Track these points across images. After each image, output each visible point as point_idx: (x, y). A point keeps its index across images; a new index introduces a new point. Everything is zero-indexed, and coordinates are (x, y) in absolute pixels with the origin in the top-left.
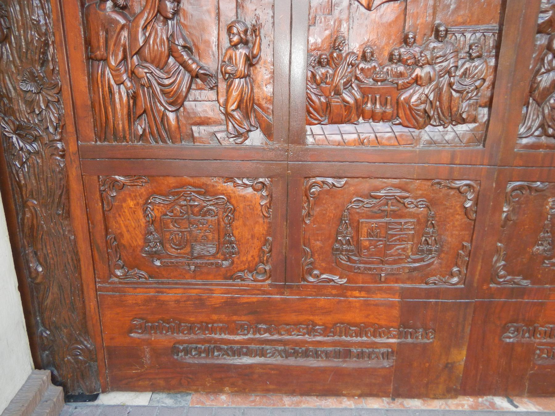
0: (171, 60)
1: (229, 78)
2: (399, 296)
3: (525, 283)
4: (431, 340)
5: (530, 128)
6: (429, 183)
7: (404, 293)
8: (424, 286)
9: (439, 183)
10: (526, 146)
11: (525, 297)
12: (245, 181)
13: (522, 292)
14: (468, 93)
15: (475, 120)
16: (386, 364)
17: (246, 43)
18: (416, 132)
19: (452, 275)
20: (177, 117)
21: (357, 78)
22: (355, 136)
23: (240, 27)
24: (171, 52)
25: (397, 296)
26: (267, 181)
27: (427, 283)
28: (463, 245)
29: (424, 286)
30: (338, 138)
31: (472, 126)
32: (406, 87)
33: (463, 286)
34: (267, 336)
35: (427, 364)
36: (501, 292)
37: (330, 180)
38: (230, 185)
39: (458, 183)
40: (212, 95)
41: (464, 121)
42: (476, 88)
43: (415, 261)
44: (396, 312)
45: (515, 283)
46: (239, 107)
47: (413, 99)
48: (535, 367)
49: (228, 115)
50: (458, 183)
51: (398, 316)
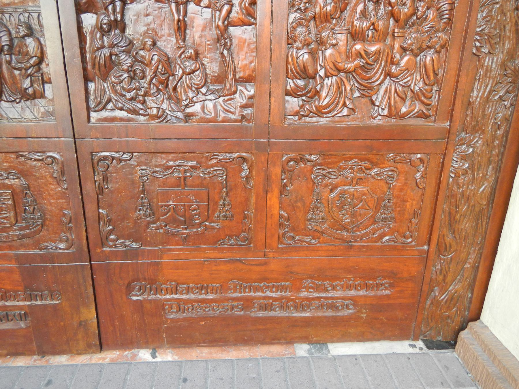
2: (16, 262)
3: (135, 245)
4: (59, 301)
5: (100, 103)
6: (13, 156)
7: (19, 259)
8: (37, 252)
9: (22, 156)
10: (99, 120)
11: (140, 258)
13: (135, 254)
14: (27, 69)
15: (42, 96)
16: (22, 325)
19: (61, 241)
25: (14, 262)
27: (41, 249)
28: (64, 213)
29: (37, 252)
33: (74, 250)
35: (62, 324)
36: (115, 255)
39: (39, 156)
41: (34, 96)
42: (32, 66)
43: (21, 229)
44: (17, 277)
45: (126, 246)
48: (168, 321)
50: (39, 156)
51: (20, 280)
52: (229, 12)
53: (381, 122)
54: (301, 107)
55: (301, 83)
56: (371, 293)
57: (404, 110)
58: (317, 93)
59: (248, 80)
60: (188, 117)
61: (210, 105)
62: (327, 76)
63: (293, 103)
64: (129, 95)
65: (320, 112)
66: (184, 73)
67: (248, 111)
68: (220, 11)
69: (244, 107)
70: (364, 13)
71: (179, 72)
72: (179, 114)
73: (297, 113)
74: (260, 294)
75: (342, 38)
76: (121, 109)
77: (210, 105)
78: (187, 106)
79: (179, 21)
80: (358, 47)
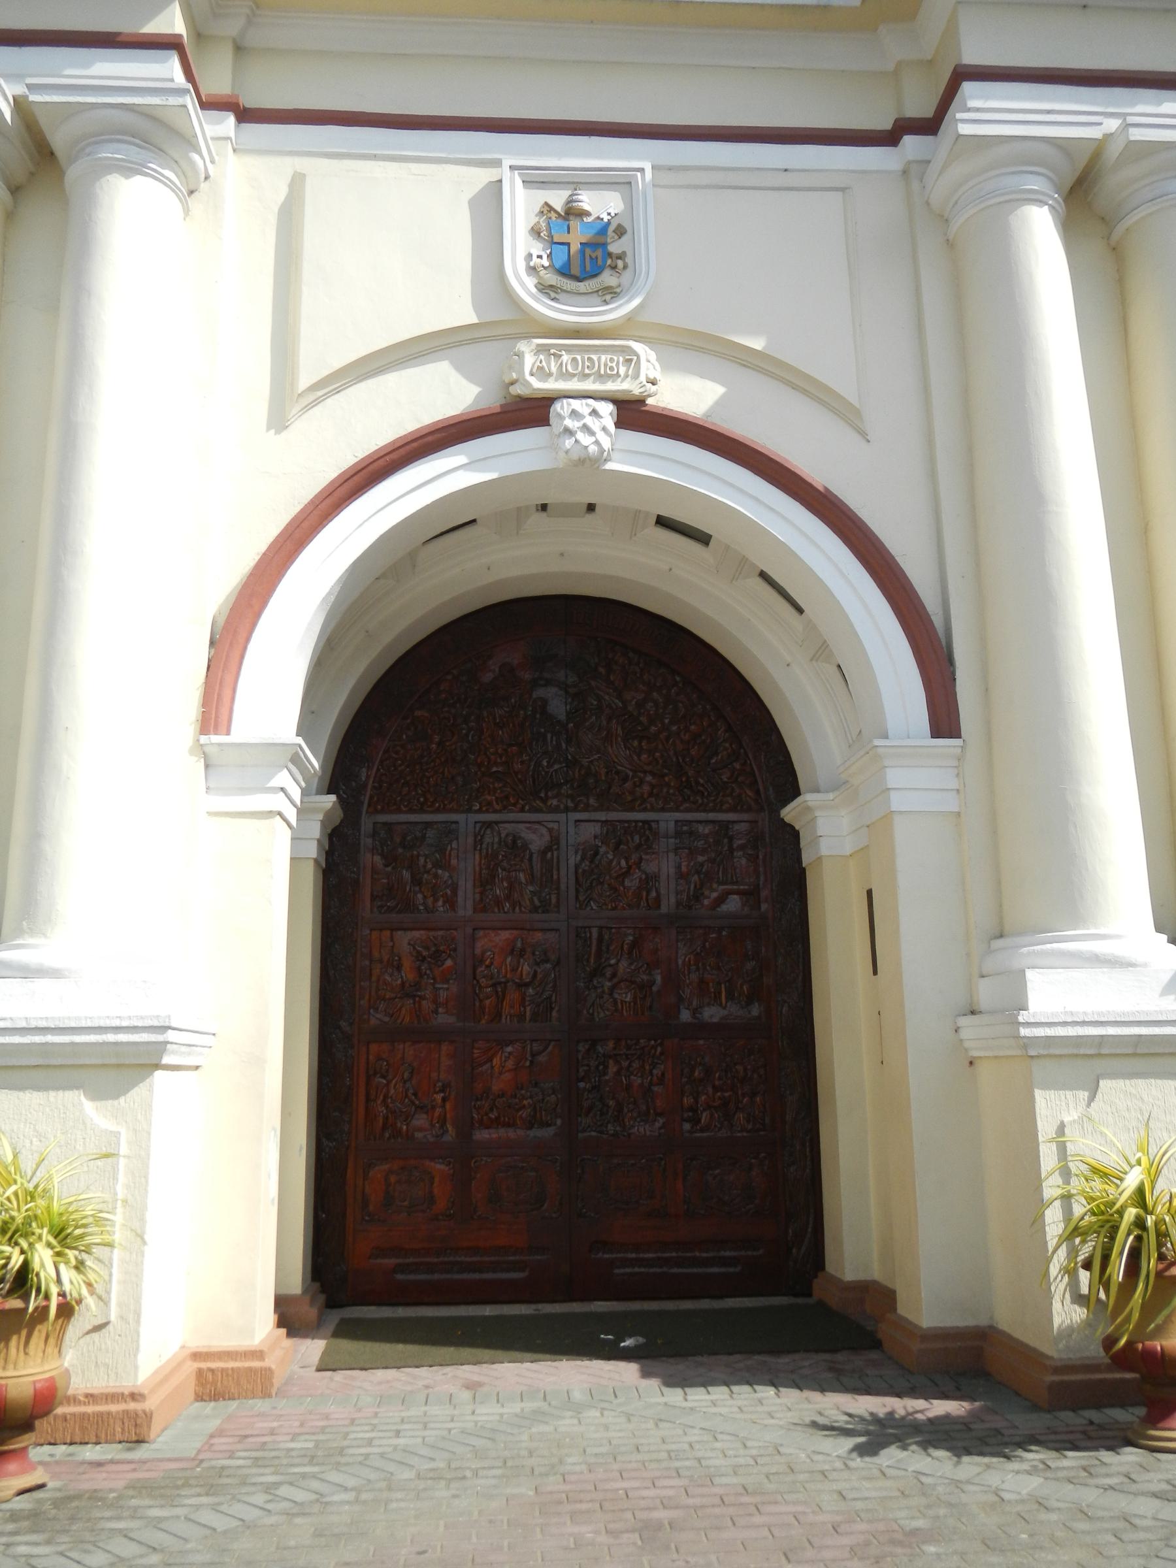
0: (407, 1100)
1: (433, 1108)
12: (440, 1160)
17: (442, 1091)
18: (528, 1132)
20: (407, 1128)
21: (496, 1106)
22: (497, 1135)
23: (440, 1084)
24: (407, 1096)
26: (452, 1160)
30: (488, 1136)
31: (554, 1127)
32: (520, 1109)
34: (451, 1259)
37: (484, 1158)
38: (432, 1164)
39: (549, 1158)
40: (425, 1116)
46: (438, 1122)
47: (524, 1115)
49: (433, 1126)
52: (651, 1079)
53: (739, 1134)
54: (692, 1127)
55: (690, 1114)
56: (749, 1253)
57: (750, 1127)
58: (699, 1121)
59: (661, 1114)
60: (629, 1135)
61: (642, 1130)
62: (704, 1110)
63: (687, 1126)
64: (599, 1123)
65: (702, 1130)
66: (628, 1111)
67: (663, 1131)
68: (647, 1079)
69: (660, 1128)
70: (720, 1078)
71: (625, 1110)
72: (626, 1134)
73: (689, 1132)
74: (674, 1254)
75: (710, 1090)
76: (594, 1131)
77: (642, 1130)
78: (630, 1129)
79: (626, 1085)
80: (719, 1094)
